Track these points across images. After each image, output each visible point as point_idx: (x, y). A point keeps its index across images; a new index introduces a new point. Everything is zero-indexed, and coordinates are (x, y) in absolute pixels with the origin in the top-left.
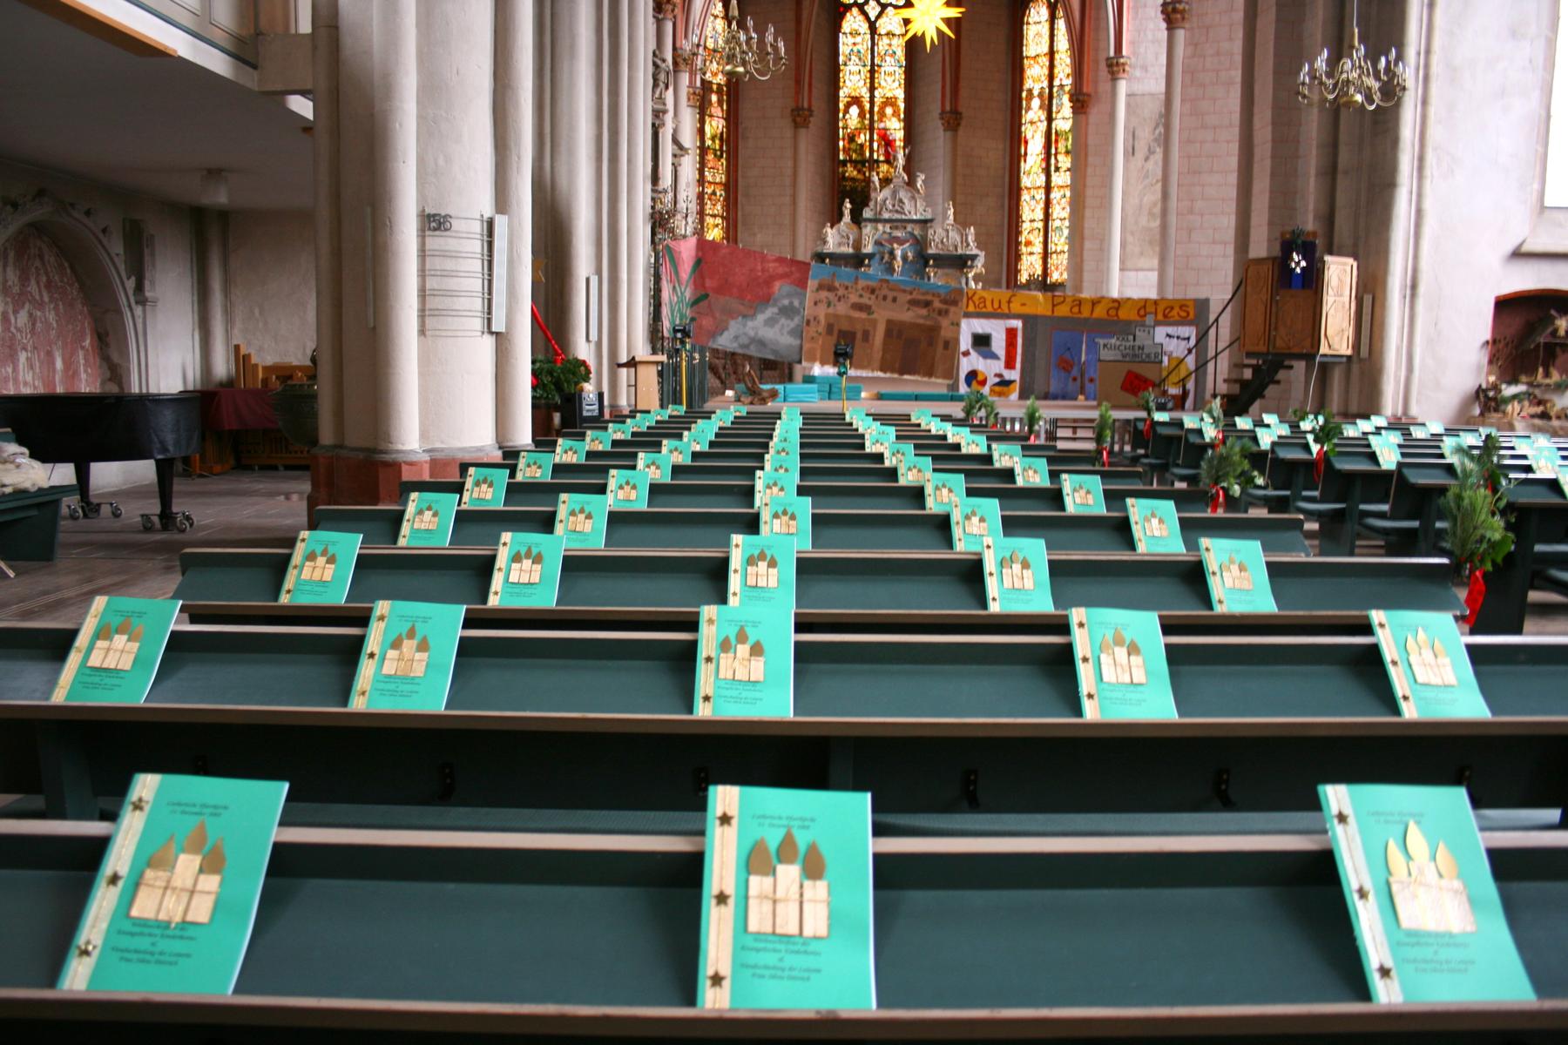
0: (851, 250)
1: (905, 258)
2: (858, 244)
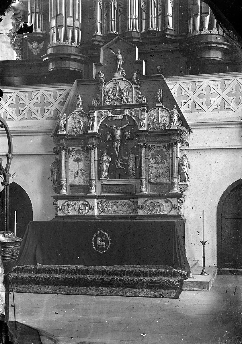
0: (81, 133)
2: (87, 128)
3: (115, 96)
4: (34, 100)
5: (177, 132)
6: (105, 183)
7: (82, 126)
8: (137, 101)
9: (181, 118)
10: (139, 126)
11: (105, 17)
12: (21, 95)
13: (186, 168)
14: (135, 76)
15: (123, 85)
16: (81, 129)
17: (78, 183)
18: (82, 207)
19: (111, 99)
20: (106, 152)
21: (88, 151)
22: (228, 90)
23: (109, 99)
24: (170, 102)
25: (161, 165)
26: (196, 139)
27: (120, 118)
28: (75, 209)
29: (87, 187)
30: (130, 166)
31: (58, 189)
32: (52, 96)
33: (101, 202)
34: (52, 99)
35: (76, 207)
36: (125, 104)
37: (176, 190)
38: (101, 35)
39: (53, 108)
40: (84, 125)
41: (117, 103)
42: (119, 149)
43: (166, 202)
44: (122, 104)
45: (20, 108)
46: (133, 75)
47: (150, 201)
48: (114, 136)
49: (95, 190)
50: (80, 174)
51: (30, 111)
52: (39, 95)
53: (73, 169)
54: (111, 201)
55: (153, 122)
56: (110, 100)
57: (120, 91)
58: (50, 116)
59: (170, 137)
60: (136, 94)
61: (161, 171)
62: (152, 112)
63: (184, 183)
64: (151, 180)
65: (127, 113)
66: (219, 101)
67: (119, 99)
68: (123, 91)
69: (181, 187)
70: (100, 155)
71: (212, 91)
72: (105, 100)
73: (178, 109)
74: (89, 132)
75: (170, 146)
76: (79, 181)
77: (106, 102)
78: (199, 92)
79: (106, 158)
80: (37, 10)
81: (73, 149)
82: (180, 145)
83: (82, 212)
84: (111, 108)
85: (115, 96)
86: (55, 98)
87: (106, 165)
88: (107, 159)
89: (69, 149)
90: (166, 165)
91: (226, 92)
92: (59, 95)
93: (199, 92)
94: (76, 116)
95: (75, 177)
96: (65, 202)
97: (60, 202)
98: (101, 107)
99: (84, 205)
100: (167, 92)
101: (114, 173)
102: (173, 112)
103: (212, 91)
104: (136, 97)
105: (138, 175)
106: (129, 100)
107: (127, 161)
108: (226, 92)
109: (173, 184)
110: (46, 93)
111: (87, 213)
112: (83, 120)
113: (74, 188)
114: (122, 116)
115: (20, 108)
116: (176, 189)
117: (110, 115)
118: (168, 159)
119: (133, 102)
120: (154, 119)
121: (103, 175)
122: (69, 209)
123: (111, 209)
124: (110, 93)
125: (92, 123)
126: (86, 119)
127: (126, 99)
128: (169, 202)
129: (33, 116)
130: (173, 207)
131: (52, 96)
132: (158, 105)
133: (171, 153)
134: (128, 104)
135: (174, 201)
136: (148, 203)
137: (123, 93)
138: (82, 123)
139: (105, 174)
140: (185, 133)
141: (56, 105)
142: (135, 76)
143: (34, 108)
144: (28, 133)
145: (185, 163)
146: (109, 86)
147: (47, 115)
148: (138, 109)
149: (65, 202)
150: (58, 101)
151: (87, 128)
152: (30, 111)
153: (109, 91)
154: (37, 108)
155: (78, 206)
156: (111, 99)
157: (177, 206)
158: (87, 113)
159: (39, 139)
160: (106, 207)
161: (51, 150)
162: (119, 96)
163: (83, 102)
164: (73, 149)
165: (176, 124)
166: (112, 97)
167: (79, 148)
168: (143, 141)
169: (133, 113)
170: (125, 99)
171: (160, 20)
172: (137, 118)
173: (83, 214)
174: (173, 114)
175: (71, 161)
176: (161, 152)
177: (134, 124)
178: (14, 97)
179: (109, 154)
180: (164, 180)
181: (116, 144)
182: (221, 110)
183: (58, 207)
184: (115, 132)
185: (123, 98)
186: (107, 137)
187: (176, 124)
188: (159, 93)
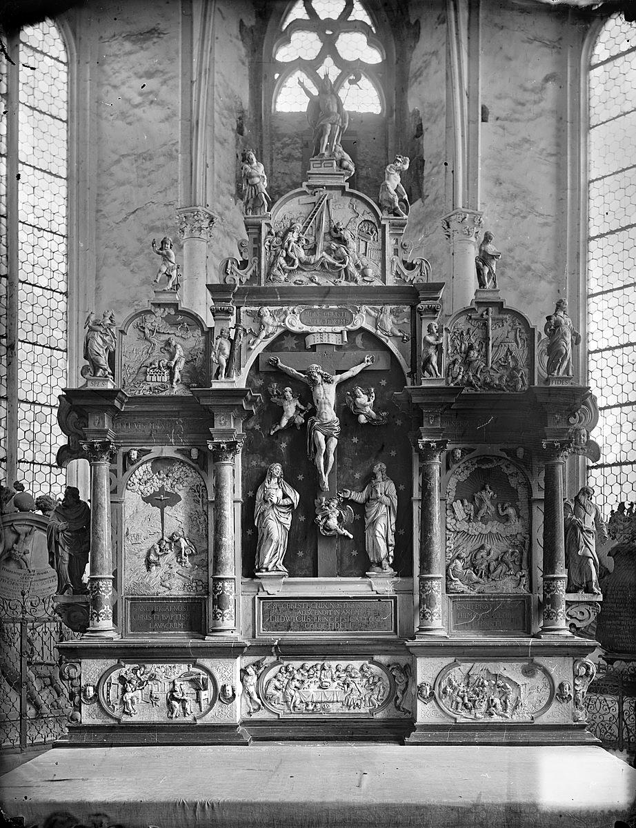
0: (178, 390)
1: (347, 412)
3: (313, 251)
7: (181, 366)
16: (177, 375)
17: (162, 589)
18: (185, 689)
19: (297, 261)
20: (277, 469)
21: (206, 461)
23: (289, 259)
27: (334, 340)
28: (152, 699)
29: (199, 611)
33: (257, 665)
35: (160, 690)
36: (352, 284)
40: (187, 363)
41: (324, 281)
42: (332, 459)
43: (528, 672)
44: (344, 283)
47: (465, 667)
49: (233, 623)
54: (297, 664)
55: (467, 363)
56: (295, 267)
57: (336, 236)
60: (396, 252)
61: (495, 548)
64: (459, 585)
65: (362, 320)
67: (329, 264)
68: (347, 235)
70: (254, 482)
74: (216, 385)
77: (278, 273)
79: (280, 494)
81: (142, 453)
83: (184, 708)
87: (282, 520)
88: (285, 496)
89: (127, 455)
95: (149, 564)
101: (305, 548)
104: (397, 260)
106: (370, 272)
107: (361, 508)
111: (207, 713)
114: (341, 332)
117: (297, 325)
119: (384, 280)
120: (471, 347)
121: (266, 561)
122: (128, 696)
123: (297, 694)
124: (293, 237)
125: (227, 351)
127: (357, 266)
128: (539, 674)
133: (539, 481)
134: (364, 284)
136: (457, 674)
137: (343, 241)
138: (179, 352)
140: (585, 407)
153: (290, 230)
155: (168, 687)
156: (297, 261)
157: (572, 687)
160: (276, 688)
162: (329, 250)
164: (142, 453)
166: (302, 254)
167: (168, 452)
170: (352, 268)
173: (189, 719)
175: (132, 500)
179: (289, 478)
181: (321, 437)
183: (83, 691)
184: (319, 391)
185: (344, 263)
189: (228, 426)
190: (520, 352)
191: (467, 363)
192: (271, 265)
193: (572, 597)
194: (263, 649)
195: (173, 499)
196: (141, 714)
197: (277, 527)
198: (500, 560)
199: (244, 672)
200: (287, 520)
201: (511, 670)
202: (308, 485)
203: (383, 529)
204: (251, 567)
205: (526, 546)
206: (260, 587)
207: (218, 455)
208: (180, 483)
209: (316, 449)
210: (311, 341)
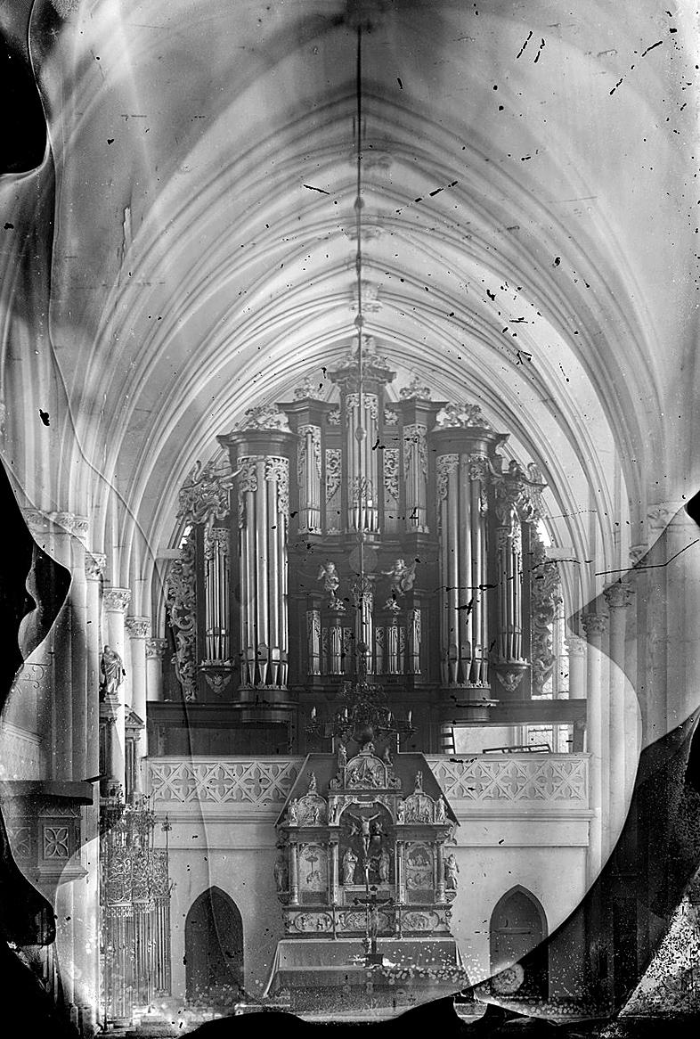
0: (317, 825)
2: (324, 819)
4: (246, 776)
5: (445, 828)
6: (350, 889)
8: (390, 785)
9: (448, 810)
10: (394, 817)
11: (324, 648)
12: (227, 767)
13: (455, 872)
14: (387, 753)
15: (371, 763)
18: (322, 921)
20: (350, 850)
21: (327, 847)
22: (503, 773)
24: (434, 791)
25: (422, 867)
26: (464, 833)
27: (368, 806)
28: (311, 924)
29: (324, 896)
30: (384, 869)
31: (286, 900)
32: (270, 771)
33: (344, 914)
34: (270, 775)
35: (314, 921)
37: (443, 900)
38: (319, 674)
39: (273, 787)
43: (431, 915)
45: (225, 785)
46: (385, 752)
47: (411, 913)
48: (361, 830)
49: (337, 899)
50: (316, 877)
51: (240, 789)
52: (252, 769)
53: (307, 869)
54: (357, 914)
55: (412, 813)
58: (268, 797)
59: (433, 834)
61: (422, 875)
62: (410, 800)
63: (451, 890)
64: (410, 887)
65: (377, 800)
66: (491, 788)
68: (373, 772)
69: (448, 895)
70: (342, 853)
71: (484, 774)
72: (348, 782)
73: (444, 798)
74: (330, 825)
75: (435, 845)
76: (315, 886)
78: (467, 774)
80: (223, 632)
81: (306, 844)
82: (446, 843)
84: (357, 793)
85: (361, 777)
86: (276, 773)
90: (429, 867)
91: (500, 776)
92: (280, 771)
93: (467, 774)
94: (308, 801)
95: (308, 881)
96: (299, 915)
97: (292, 915)
98: (343, 790)
99: (325, 919)
100: (428, 774)
101: (359, 877)
102: (439, 804)
103: (484, 774)
105: (392, 879)
107: (378, 862)
108: (500, 776)
109: (439, 892)
110: (263, 767)
112: (319, 807)
113: (307, 896)
115: (225, 785)
116: (443, 899)
117: (356, 801)
118: (431, 860)
119: (385, 786)
124: (355, 773)
126: (322, 806)
128: (435, 916)
129: (244, 796)
130: (441, 922)
131: (270, 771)
132: (417, 791)
133: (435, 852)
135: (442, 914)
136: (408, 915)
139: (349, 878)
141: (277, 783)
142: (387, 753)
143: (245, 787)
144: (184, 819)
145: (453, 865)
146: (354, 762)
147: (264, 796)
148: (392, 795)
149: (299, 915)
150: (279, 779)
151: (324, 819)
152: (240, 789)
153: (354, 770)
154: (249, 786)
158: (325, 795)
159: (252, 827)
161: (274, 842)
162: (366, 777)
163: (317, 782)
164: (306, 844)
165: (442, 819)
167: (314, 844)
168: (294, 840)
169: (386, 800)
171: (402, 658)
172: (391, 807)
174: (439, 806)
175: (302, 859)
176: (422, 852)
177: (387, 818)
178: (216, 769)
179: (353, 852)
180: (426, 887)
182: (494, 799)
183: (290, 922)
186: (351, 830)
187: (442, 819)
188: (419, 776)
189: (334, 837)
190: (430, 810)
191: (412, 813)
192: (348, 782)
193: (447, 891)
194: (347, 908)
195: (316, 859)
196: (308, 930)
197: (351, 868)
198: (424, 878)
199: (340, 916)
200: (354, 866)
201: (426, 914)
202: (361, 855)
203: (385, 869)
204: (341, 881)
205: (432, 873)
206: (345, 888)
207: (332, 846)
208: (318, 854)
209: (363, 843)
210: (360, 806)
